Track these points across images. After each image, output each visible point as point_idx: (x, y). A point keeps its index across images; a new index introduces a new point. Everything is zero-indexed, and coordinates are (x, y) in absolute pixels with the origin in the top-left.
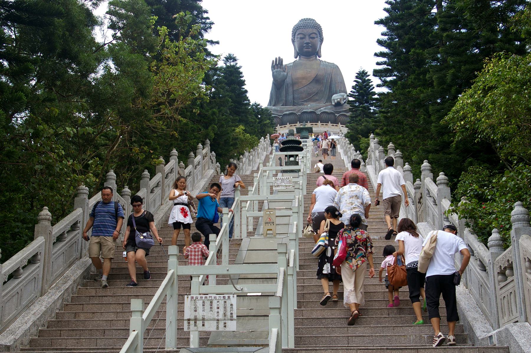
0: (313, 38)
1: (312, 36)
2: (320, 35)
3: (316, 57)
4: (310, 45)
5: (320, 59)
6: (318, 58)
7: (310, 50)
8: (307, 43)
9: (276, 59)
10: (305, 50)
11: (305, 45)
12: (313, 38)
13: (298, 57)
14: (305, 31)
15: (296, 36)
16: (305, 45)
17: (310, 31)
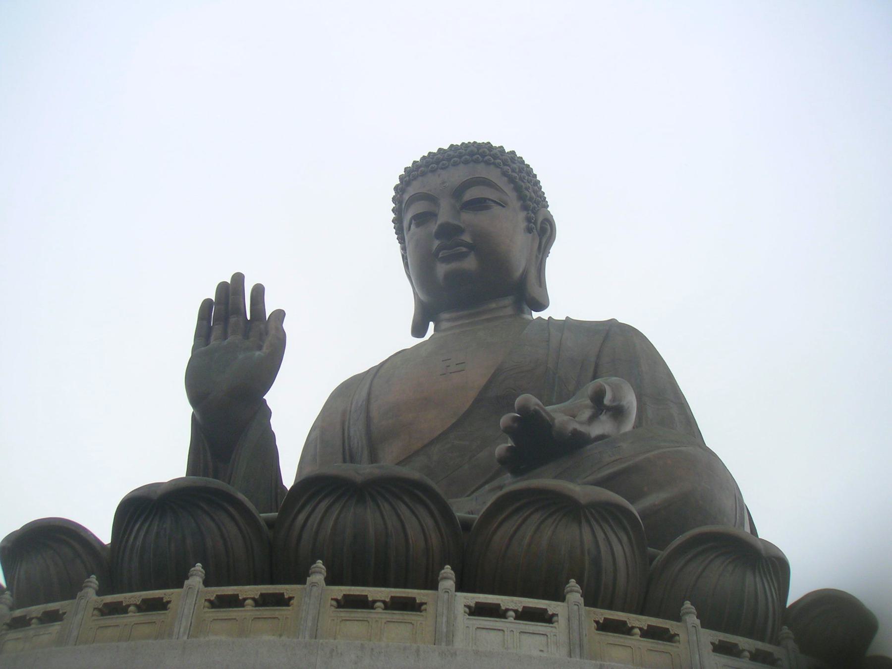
0: (479, 205)
1: (469, 195)
2: (521, 197)
3: (519, 310)
4: (467, 238)
5: (544, 315)
6: (535, 315)
7: (470, 263)
8: (449, 232)
9: (223, 288)
10: (442, 269)
11: (436, 243)
12: (479, 205)
13: (432, 325)
14: (432, 183)
15: (406, 224)
16: (436, 243)
17: (458, 175)
